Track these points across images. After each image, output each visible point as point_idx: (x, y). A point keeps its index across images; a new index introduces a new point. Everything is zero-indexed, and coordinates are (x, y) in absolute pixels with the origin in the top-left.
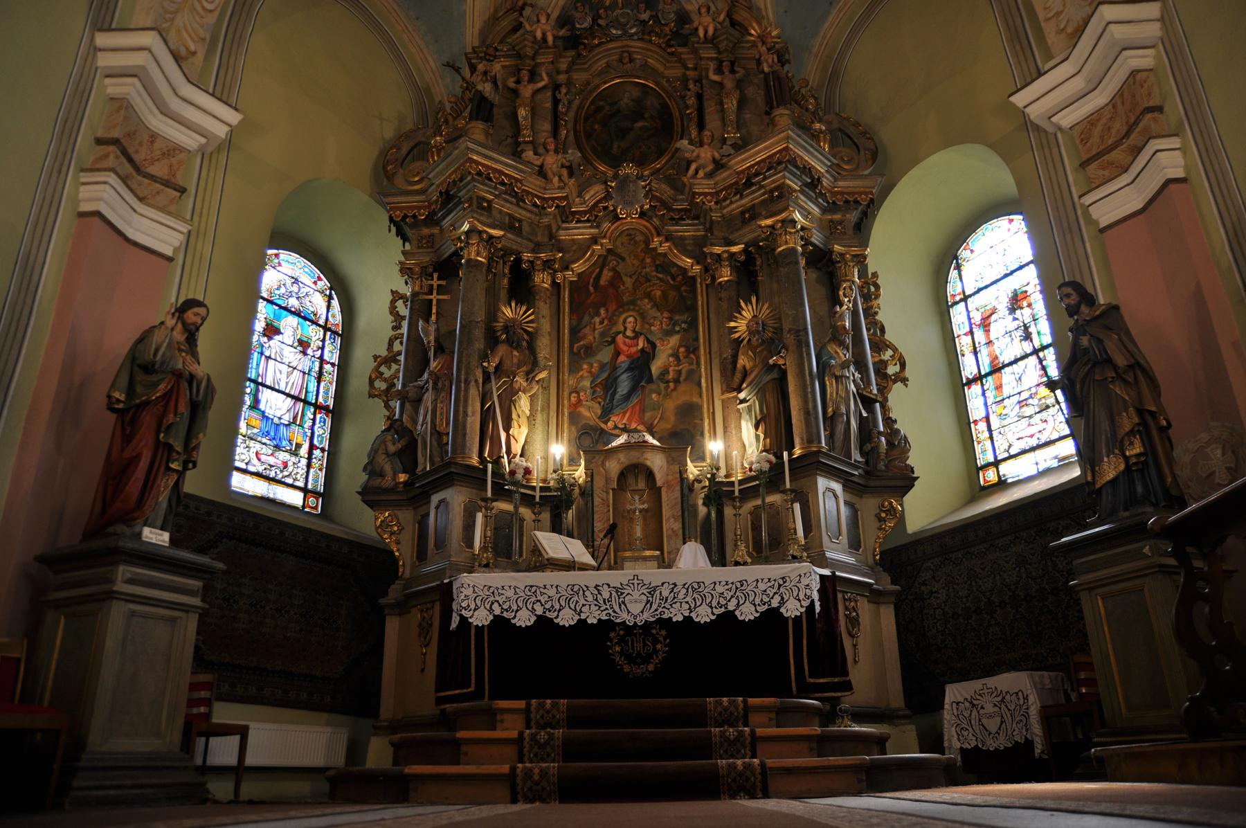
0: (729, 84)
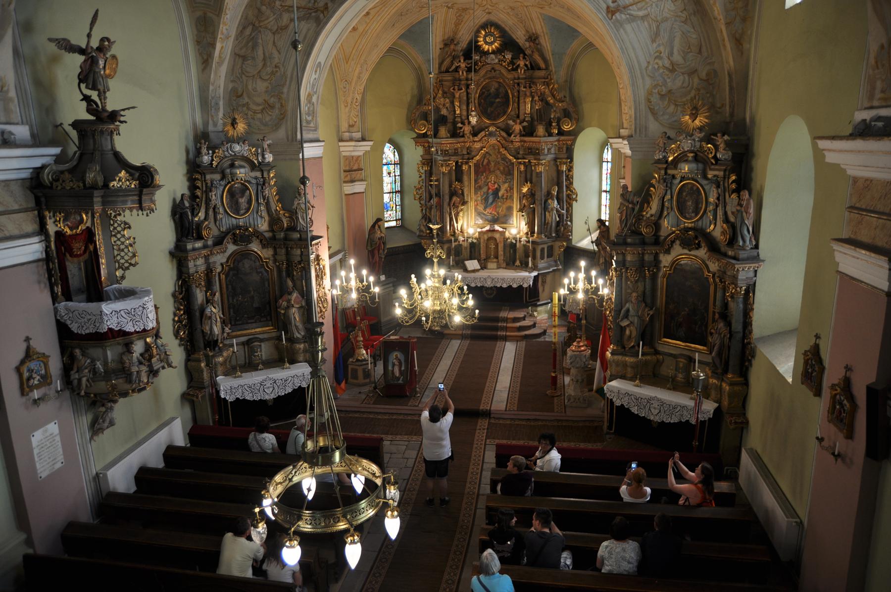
0: (528, 94)
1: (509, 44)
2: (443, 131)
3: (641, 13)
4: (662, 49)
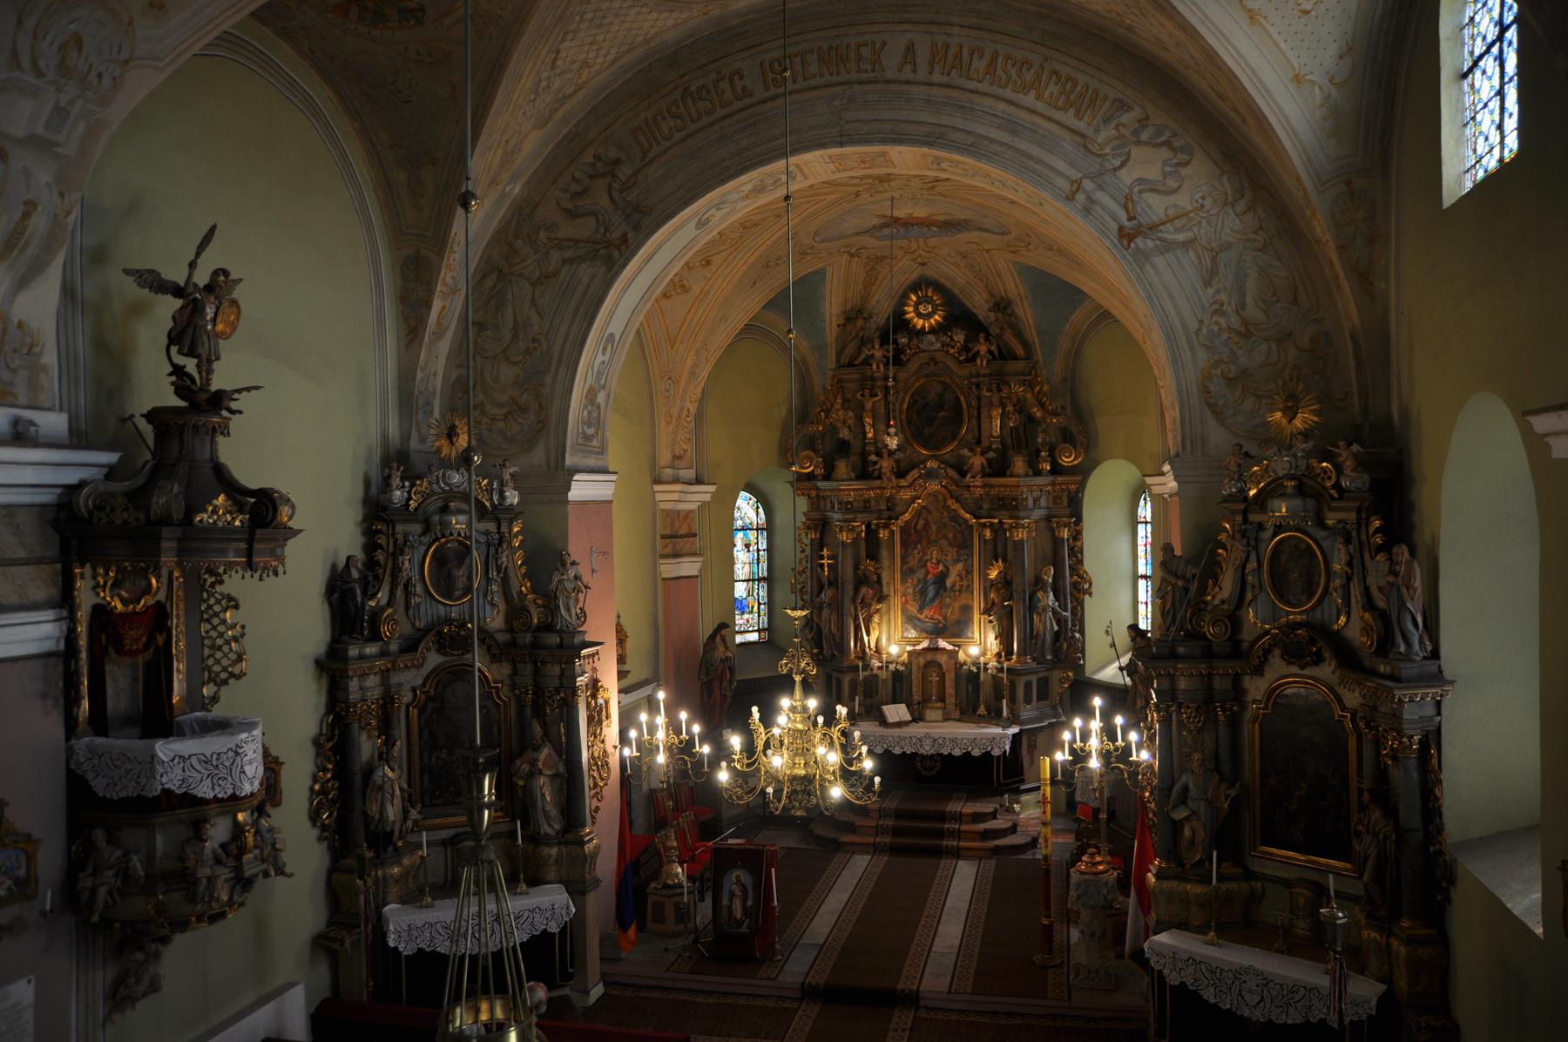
0: (996, 401)
1: (959, 317)
2: (842, 467)
3: (1181, 237)
4: (1224, 297)
